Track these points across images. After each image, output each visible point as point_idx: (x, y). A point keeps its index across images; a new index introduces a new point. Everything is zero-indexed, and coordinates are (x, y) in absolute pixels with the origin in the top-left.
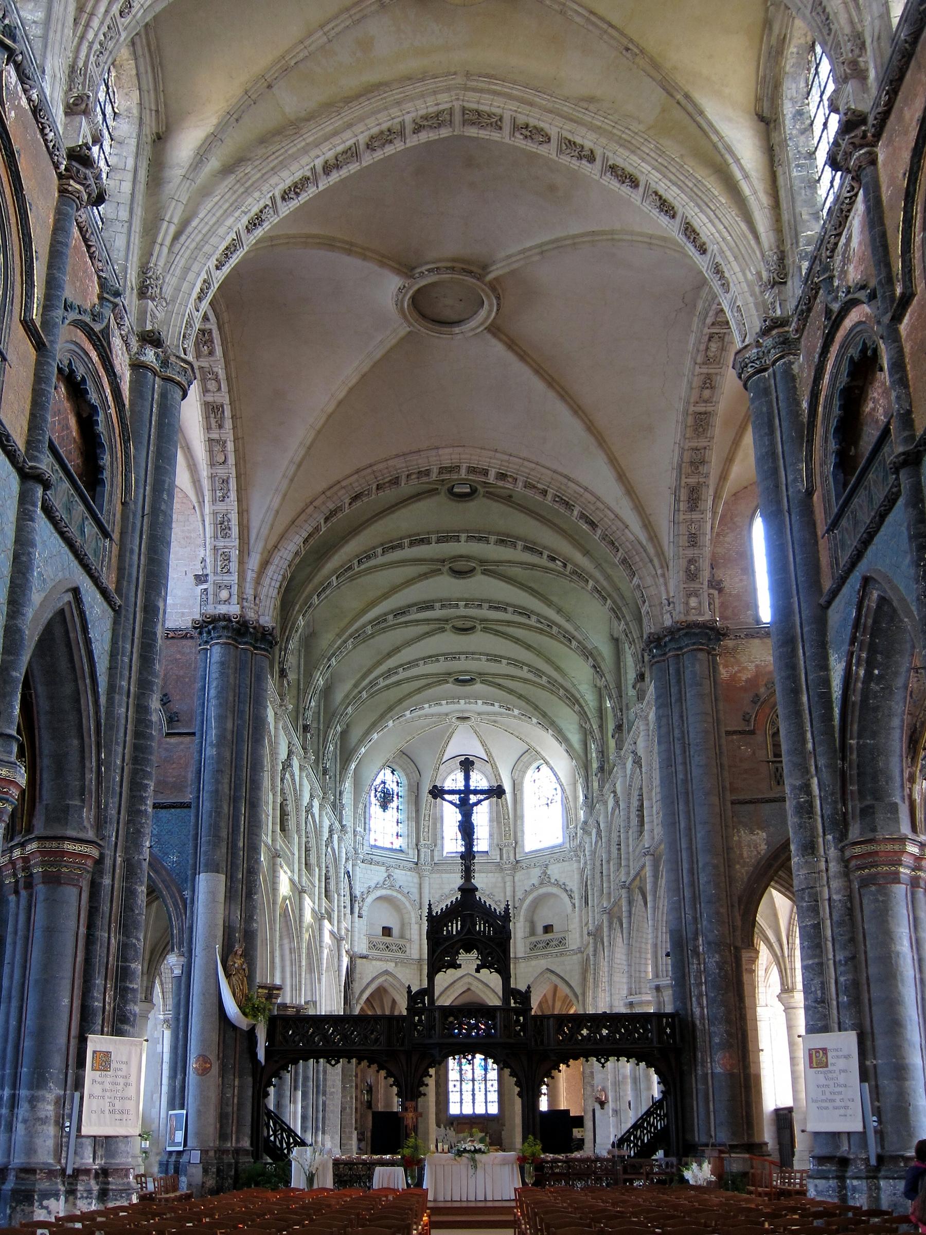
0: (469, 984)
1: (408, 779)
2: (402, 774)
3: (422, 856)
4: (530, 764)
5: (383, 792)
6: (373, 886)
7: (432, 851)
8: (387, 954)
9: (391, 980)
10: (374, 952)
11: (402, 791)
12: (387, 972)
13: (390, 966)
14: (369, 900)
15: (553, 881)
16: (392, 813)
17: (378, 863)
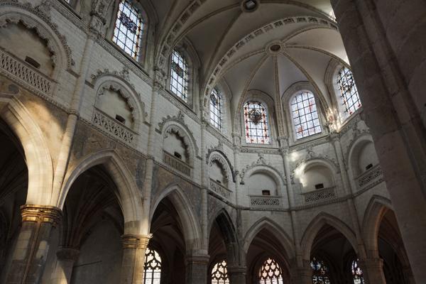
0: (324, 219)
1: (268, 105)
2: (264, 104)
3: (281, 144)
4: (333, 72)
5: (254, 114)
6: (250, 165)
7: (287, 140)
8: (265, 206)
9: (269, 223)
10: (256, 206)
11: (265, 113)
12: (266, 218)
13: (268, 214)
14: (249, 173)
15: (362, 132)
16: (259, 126)
17: (251, 152)
